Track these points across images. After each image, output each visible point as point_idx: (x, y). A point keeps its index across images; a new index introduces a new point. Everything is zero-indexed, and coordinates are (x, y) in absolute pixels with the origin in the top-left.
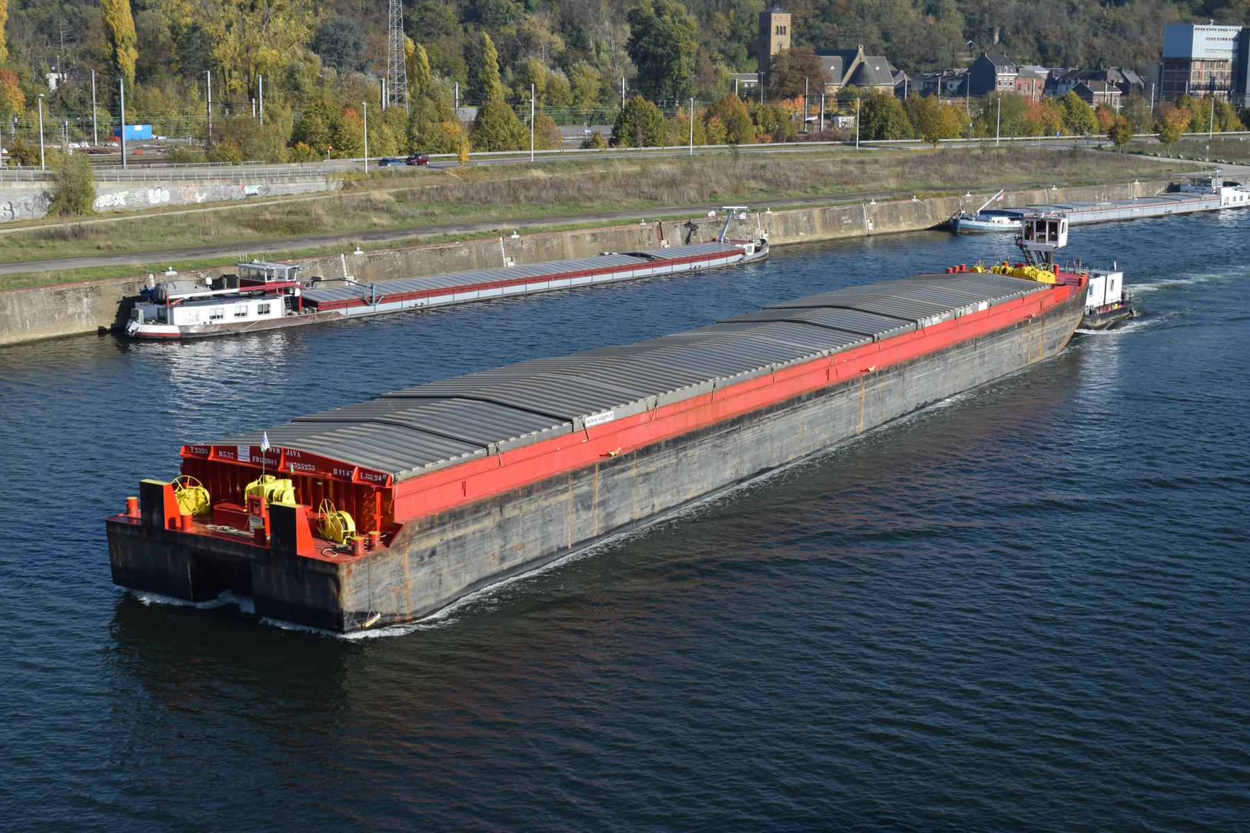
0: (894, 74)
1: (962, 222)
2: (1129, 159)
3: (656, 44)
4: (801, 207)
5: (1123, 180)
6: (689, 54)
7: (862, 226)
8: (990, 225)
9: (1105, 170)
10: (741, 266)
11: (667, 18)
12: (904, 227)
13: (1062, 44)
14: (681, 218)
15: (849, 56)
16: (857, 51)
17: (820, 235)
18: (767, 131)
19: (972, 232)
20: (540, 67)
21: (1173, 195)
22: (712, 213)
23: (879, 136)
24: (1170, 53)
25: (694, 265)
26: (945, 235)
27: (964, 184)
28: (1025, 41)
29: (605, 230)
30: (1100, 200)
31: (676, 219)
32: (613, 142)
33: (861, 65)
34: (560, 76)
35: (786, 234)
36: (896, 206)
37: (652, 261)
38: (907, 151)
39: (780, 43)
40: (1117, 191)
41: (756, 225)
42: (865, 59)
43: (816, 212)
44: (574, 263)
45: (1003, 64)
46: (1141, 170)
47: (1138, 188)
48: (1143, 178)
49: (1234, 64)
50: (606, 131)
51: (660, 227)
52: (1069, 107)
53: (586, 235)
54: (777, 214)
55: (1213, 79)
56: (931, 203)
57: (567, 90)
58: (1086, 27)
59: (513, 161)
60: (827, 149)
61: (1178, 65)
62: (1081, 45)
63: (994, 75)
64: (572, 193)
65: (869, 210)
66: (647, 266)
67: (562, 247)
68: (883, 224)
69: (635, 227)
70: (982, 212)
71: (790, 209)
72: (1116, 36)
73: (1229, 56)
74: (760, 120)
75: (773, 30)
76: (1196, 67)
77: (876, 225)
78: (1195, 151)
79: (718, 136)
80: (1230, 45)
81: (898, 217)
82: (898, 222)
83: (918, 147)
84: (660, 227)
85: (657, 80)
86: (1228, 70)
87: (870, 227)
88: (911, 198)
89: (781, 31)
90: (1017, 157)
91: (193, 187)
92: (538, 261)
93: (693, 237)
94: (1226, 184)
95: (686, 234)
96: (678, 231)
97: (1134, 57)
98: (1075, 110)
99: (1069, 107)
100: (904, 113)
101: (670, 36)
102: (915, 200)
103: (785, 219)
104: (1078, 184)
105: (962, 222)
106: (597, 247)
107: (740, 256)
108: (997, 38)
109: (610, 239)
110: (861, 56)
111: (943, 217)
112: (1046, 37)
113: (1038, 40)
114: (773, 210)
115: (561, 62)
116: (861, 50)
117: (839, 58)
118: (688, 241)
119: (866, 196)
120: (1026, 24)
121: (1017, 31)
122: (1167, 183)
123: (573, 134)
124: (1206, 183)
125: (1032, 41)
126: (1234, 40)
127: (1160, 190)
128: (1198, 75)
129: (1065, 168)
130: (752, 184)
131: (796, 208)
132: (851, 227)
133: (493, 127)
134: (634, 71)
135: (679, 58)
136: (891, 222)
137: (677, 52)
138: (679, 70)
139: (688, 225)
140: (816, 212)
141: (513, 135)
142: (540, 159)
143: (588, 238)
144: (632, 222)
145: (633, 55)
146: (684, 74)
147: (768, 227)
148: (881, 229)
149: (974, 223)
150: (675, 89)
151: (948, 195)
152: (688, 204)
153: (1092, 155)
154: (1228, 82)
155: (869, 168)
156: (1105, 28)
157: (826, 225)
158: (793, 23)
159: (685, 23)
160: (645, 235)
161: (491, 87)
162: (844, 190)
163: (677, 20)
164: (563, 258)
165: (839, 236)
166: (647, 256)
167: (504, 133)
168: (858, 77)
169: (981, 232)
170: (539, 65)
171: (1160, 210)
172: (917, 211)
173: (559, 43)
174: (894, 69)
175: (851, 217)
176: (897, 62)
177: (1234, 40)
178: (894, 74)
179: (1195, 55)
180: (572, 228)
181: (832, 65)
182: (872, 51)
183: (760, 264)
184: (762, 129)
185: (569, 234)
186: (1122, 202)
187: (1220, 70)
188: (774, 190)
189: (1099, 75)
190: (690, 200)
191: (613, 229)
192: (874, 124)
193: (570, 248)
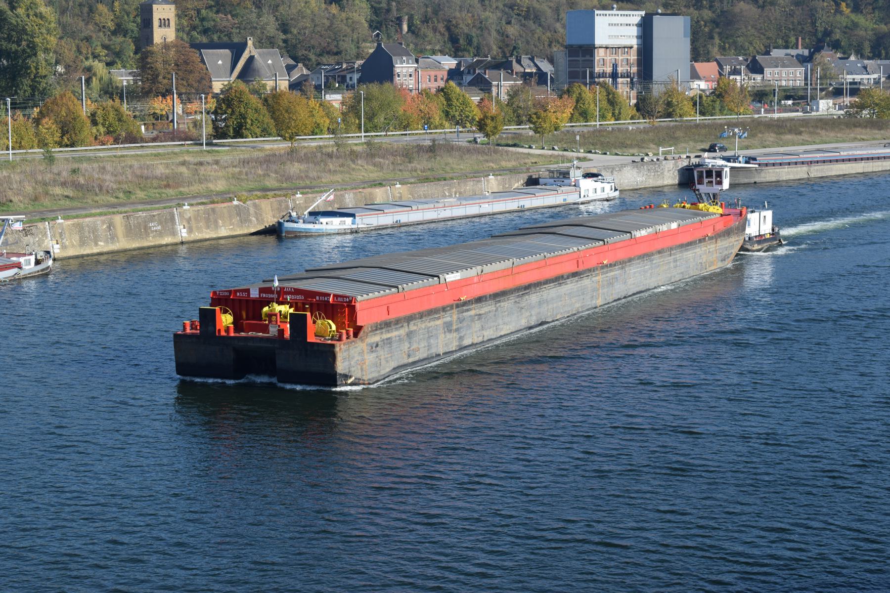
0: (290, 69)
1: (287, 225)
2: (496, 152)
3: (9, 39)
4: (101, 214)
5: (477, 174)
6: (46, 50)
7: (174, 233)
8: (317, 226)
9: (467, 164)
10: (17, 281)
11: (21, 11)
12: (223, 232)
13: (474, 33)
15: (238, 50)
16: (244, 45)
17: (123, 243)
18: (108, 133)
19: (297, 235)
21: (531, 189)
23: (238, 134)
24: (576, 41)
26: (271, 239)
27: (302, 184)
28: (435, 30)
30: (444, 196)
33: (251, 59)
35: (83, 243)
36: (213, 210)
38: (261, 150)
39: (164, 34)
40: (469, 186)
41: (45, 234)
42: (255, 53)
43: (118, 219)
45: (400, 55)
46: (504, 164)
47: (493, 182)
48: (498, 172)
49: (639, 51)
52: (448, 99)
54: (70, 222)
55: (615, 66)
56: (255, 206)
58: (499, 14)
60: (170, 150)
61: (584, 51)
62: (494, 34)
63: (392, 67)
65: (181, 215)
68: (199, 229)
70: (311, 214)
71: (86, 216)
72: (531, 24)
73: (634, 42)
74: (100, 120)
75: (156, 23)
76: (600, 54)
77: (190, 231)
78: (568, 142)
79: (50, 140)
80: (634, 31)
81: (216, 222)
82: (217, 227)
83: (275, 145)
85: (13, 78)
86: (633, 57)
87: (183, 234)
88: (231, 200)
89: (164, 23)
90: (372, 153)
94: (588, 175)
97: (550, 45)
98: (455, 102)
99: (448, 99)
100: (264, 110)
101: (24, 31)
102: (235, 203)
103: (80, 228)
104: (426, 180)
105: (287, 225)
107: (16, 270)
108: (405, 27)
110: (251, 49)
111: (270, 220)
112: (456, 26)
113: (448, 29)
114: (64, 218)
116: (250, 43)
117: (227, 51)
120: (436, 12)
121: (426, 20)
122: (523, 178)
124: (565, 175)
125: (442, 30)
126: (638, 25)
127: (518, 183)
128: (602, 62)
129: (421, 164)
130: (58, 191)
131: (94, 215)
132: (160, 234)
135: (35, 55)
136: (208, 227)
138: (37, 69)
140: (118, 219)
146: (43, 72)
147: (59, 237)
149: (301, 225)
150: (33, 88)
151: (275, 196)
153: (469, 151)
154: (634, 69)
155: (202, 170)
156: (518, 15)
157: (130, 232)
158: (178, 16)
159: (42, 17)
162: (164, 192)
163: (31, 13)
165: (146, 244)
169: (308, 235)
171: (512, 205)
172: (239, 214)
174: (292, 62)
175: (160, 223)
176: (294, 52)
177: (638, 25)
178: (290, 69)
179: (598, 42)
181: (218, 59)
182: (266, 42)
183: (44, 276)
184: (102, 130)
186: (476, 196)
187: (625, 57)
188: (82, 195)
189: (503, 65)
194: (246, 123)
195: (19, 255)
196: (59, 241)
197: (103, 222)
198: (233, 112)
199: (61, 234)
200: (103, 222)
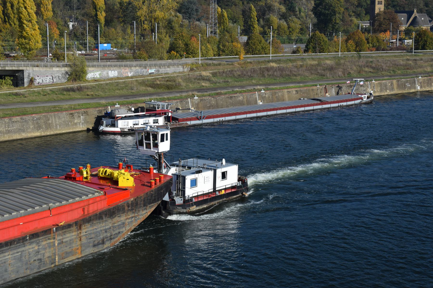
3: (325, 9)
4: (388, 79)
6: (339, 13)
7: (415, 88)
10: (360, 104)
14: (335, 84)
15: (410, 14)
16: (414, 11)
17: (396, 91)
20: (275, 19)
22: (348, 82)
23: (423, 48)
25: (340, 104)
29: (302, 89)
31: (333, 84)
32: (306, 51)
33: (415, 17)
34: (284, 23)
35: (381, 91)
36: (430, 79)
37: (322, 102)
41: (368, 87)
42: (417, 15)
43: (395, 82)
44: (288, 102)
50: (303, 46)
51: (325, 88)
53: (294, 91)
54: (377, 82)
57: (286, 29)
59: (263, 59)
60: (400, 54)
64: (288, 73)
65: (418, 81)
66: (319, 104)
67: (283, 96)
68: (425, 87)
69: (315, 88)
71: (383, 80)
74: (370, 42)
75: (377, 3)
77: (421, 87)
79: (351, 48)
84: (325, 88)
91: (127, 70)
92: (272, 102)
93: (340, 92)
95: (337, 91)
96: (333, 90)
101: (331, 6)
103: (381, 84)
106: (298, 96)
107: (360, 100)
109: (304, 93)
110: (415, 14)
114: (375, 80)
115: (283, 17)
116: (415, 11)
117: (406, 14)
118: (338, 93)
119: (417, 75)
123: (288, 48)
130: (366, 69)
131: (386, 80)
132: (410, 88)
133: (254, 45)
134: (315, 20)
135: (335, 15)
136: (428, 86)
137: (334, 12)
138: (335, 20)
139: (338, 86)
140: (395, 82)
141: (263, 48)
142: (274, 58)
143: (294, 92)
144: (313, 86)
145: (315, 14)
146: (338, 22)
148: (424, 89)
150: (333, 28)
152: (338, 78)
157: (399, 87)
160: (319, 91)
161: (254, 27)
162: (408, 72)
164: (283, 100)
165: (404, 92)
166: (320, 100)
167: (259, 47)
168: (414, 22)
170: (275, 18)
173: (283, 9)
174: (430, 19)
180: (287, 88)
181: (402, 17)
182: (420, 11)
184: (371, 45)
185: (286, 90)
188: (376, 72)
190: (339, 76)
191: (305, 88)
192: (421, 43)
193: (286, 96)
194: (427, 44)
195: (362, 94)
196: (371, 90)
197: (389, 83)
198: (422, 40)
199: (374, 87)
200: (389, 83)
